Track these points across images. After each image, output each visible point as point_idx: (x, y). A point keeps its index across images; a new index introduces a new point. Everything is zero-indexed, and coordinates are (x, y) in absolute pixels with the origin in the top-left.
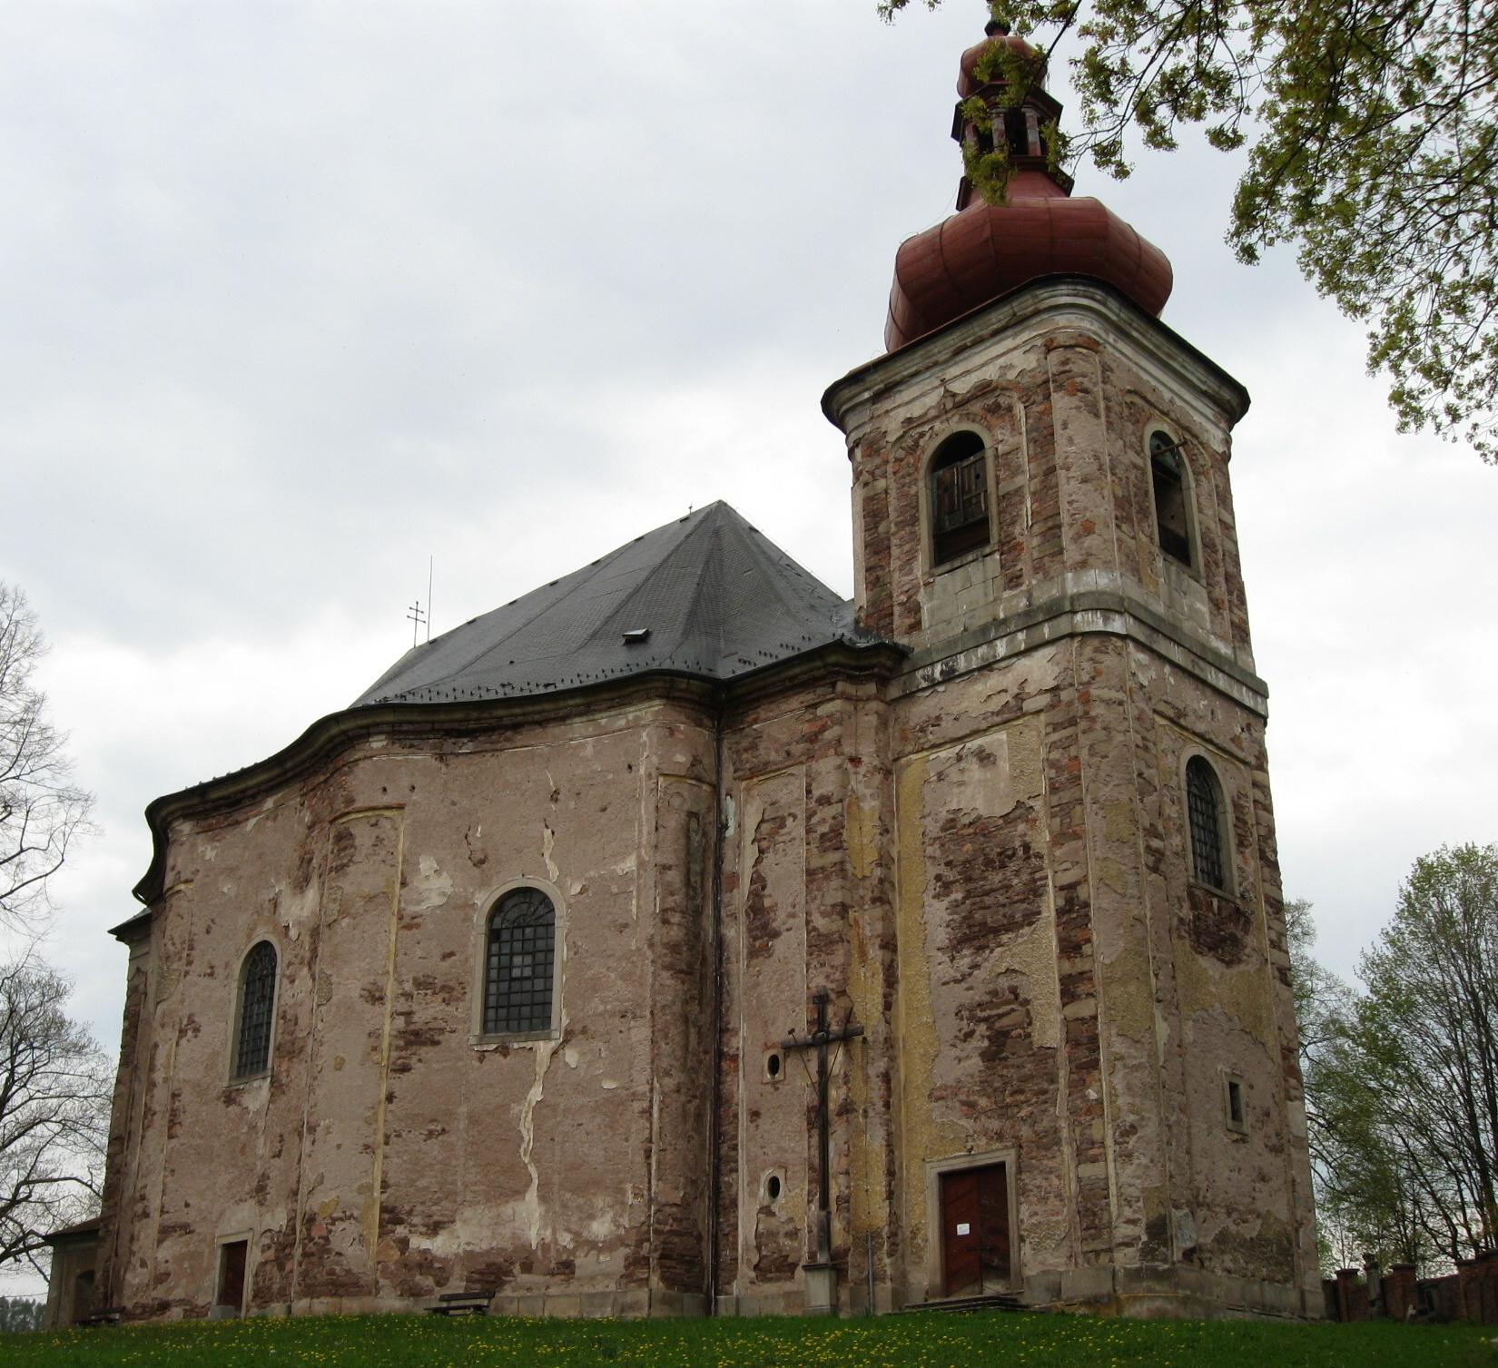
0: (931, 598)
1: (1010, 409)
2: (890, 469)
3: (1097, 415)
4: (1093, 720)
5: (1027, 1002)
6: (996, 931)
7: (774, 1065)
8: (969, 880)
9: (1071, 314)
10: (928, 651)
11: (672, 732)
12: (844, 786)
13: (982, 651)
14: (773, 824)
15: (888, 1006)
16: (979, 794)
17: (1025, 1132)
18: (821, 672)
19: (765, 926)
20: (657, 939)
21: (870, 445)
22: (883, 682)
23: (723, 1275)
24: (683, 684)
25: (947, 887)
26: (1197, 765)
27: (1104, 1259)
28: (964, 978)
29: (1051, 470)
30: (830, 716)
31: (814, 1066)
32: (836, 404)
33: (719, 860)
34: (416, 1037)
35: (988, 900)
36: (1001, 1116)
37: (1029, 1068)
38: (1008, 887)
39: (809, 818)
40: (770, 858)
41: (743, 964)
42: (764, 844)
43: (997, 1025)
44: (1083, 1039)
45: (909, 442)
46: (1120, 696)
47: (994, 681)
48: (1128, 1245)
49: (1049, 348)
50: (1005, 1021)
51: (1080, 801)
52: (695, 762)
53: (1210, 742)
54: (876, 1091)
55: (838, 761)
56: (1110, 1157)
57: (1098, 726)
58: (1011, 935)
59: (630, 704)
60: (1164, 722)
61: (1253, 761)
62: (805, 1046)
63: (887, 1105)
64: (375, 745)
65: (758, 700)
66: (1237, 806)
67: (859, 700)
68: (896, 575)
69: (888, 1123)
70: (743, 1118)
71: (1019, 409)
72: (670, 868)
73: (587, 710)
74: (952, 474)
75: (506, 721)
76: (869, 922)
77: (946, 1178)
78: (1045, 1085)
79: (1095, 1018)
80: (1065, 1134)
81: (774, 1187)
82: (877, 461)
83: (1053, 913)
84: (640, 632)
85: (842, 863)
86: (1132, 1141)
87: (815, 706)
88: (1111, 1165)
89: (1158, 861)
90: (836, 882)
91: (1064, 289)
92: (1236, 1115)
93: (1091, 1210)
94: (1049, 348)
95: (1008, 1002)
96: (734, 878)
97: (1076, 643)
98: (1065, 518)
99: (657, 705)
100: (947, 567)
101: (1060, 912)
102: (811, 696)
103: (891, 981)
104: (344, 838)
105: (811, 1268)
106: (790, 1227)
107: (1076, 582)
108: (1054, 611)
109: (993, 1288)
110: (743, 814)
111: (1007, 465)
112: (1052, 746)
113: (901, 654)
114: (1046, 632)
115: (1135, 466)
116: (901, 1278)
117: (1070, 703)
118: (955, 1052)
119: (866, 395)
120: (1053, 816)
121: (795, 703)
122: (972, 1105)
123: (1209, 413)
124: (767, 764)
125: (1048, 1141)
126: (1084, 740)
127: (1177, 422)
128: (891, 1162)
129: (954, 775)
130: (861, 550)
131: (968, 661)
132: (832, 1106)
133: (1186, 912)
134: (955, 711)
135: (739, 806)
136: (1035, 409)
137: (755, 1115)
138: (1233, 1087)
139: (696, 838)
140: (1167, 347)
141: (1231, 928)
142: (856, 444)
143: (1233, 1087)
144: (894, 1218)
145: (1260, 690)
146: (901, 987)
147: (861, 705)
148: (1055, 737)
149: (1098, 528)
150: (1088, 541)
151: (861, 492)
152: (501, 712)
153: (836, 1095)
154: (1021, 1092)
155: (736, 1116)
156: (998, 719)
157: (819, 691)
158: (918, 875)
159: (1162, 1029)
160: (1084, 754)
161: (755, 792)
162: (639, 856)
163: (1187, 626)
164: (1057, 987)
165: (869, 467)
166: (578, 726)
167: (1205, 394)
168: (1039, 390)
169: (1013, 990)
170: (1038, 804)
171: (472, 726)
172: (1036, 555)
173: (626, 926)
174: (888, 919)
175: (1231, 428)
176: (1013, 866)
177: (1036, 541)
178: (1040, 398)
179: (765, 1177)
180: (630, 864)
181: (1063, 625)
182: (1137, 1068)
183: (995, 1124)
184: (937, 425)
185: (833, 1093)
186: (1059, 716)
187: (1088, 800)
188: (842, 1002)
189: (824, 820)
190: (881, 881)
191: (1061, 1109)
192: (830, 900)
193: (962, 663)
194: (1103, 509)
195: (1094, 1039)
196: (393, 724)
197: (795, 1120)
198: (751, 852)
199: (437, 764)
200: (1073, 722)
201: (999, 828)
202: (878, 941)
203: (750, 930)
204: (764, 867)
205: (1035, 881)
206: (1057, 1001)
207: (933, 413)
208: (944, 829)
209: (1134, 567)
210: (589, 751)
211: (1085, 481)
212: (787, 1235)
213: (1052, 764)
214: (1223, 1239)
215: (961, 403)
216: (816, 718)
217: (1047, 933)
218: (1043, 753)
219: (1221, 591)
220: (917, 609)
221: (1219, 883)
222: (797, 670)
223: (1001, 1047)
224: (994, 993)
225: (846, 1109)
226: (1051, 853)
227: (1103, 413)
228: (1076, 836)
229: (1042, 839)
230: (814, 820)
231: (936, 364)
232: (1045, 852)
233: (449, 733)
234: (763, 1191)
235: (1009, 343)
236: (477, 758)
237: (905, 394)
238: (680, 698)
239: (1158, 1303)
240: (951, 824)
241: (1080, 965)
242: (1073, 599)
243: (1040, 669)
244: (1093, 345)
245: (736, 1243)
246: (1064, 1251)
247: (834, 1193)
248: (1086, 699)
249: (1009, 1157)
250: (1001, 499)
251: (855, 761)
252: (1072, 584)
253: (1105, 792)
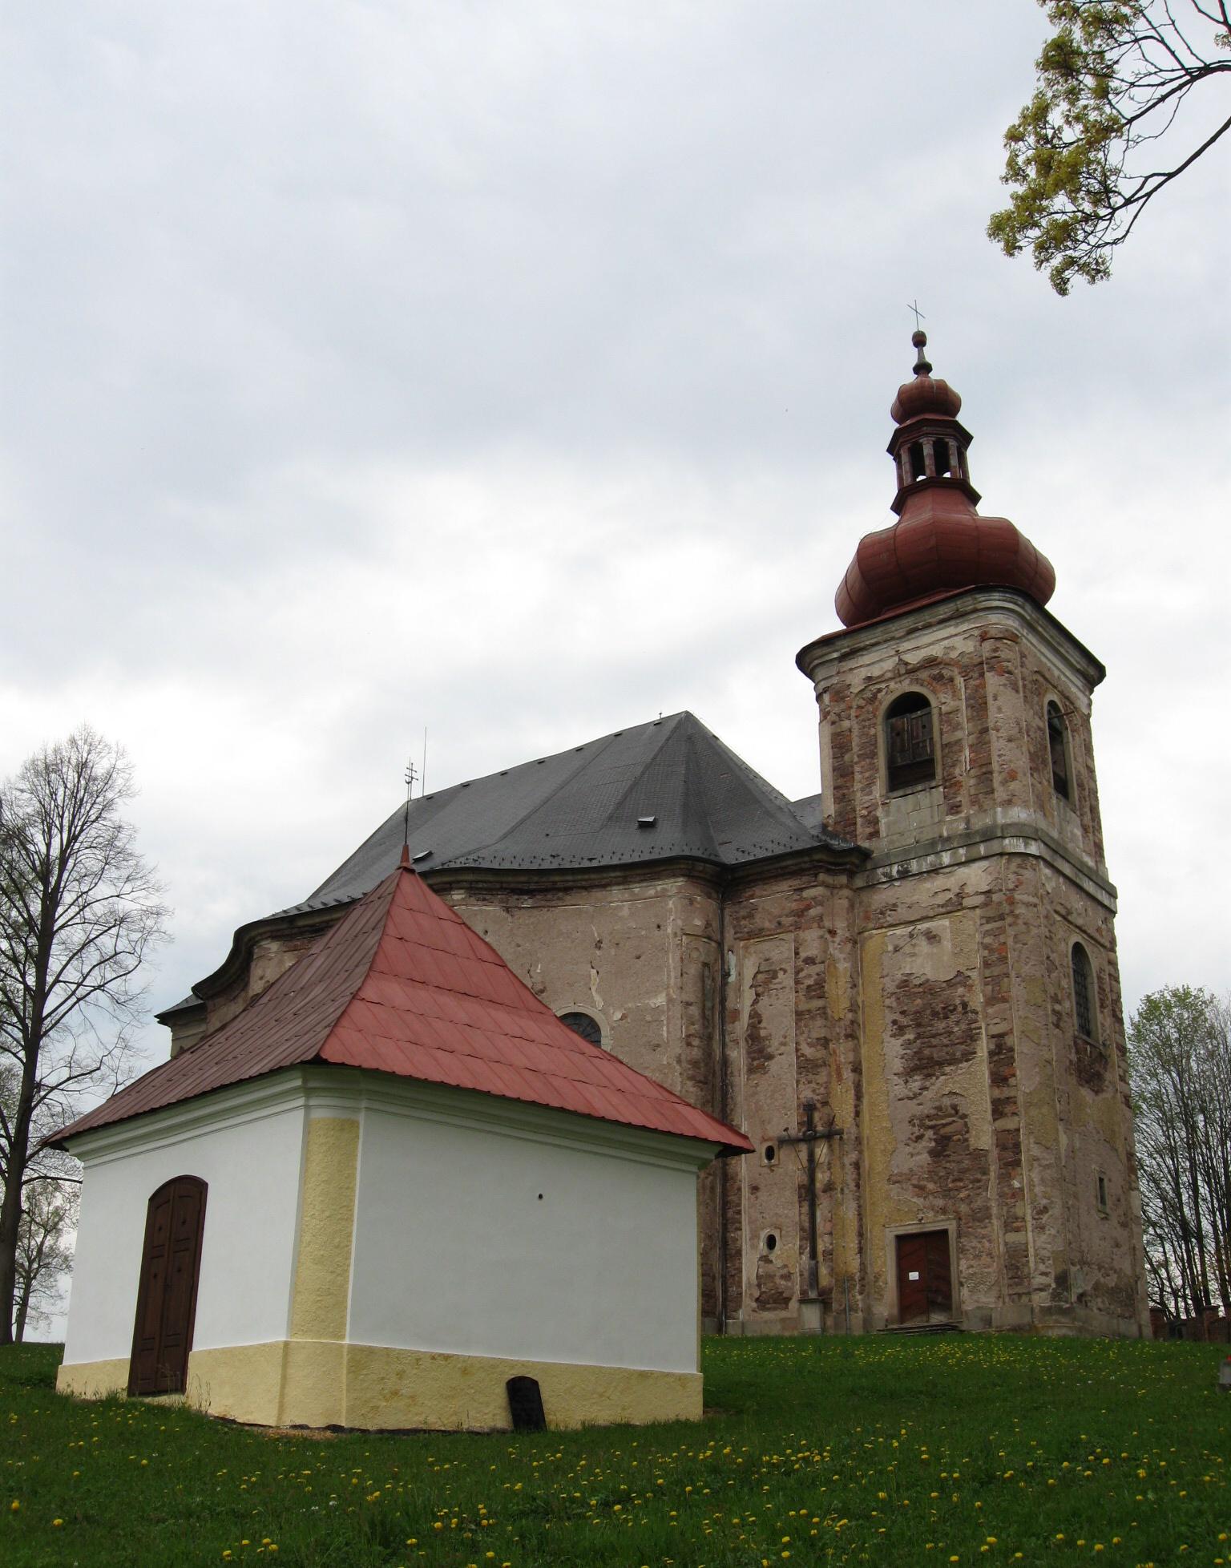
0: (888, 814)
1: (951, 680)
2: (853, 713)
3: (1017, 691)
4: (1017, 917)
5: (964, 1116)
6: (940, 1064)
7: (770, 1154)
8: (919, 1025)
9: (999, 613)
10: (888, 855)
11: (691, 902)
12: (825, 952)
13: (930, 859)
14: (766, 977)
15: (857, 1114)
16: (927, 964)
17: (963, 1208)
18: (807, 866)
19: (761, 1051)
20: (683, 1057)
21: (838, 692)
22: (851, 874)
23: (731, 1305)
24: (700, 866)
25: (901, 1030)
26: (1078, 947)
27: (1024, 1299)
28: (915, 1096)
29: (985, 730)
30: (814, 898)
31: (804, 1156)
32: (807, 660)
33: (723, 1000)
35: (934, 1041)
36: (944, 1197)
37: (967, 1163)
38: (951, 1033)
39: (797, 973)
40: (764, 1001)
41: (743, 1078)
42: (760, 990)
43: (942, 1131)
44: (1009, 1145)
45: (869, 695)
47: (939, 882)
48: (1041, 1290)
49: (984, 638)
50: (948, 1129)
51: (1007, 975)
52: (708, 925)
53: (1085, 932)
54: (850, 1176)
55: (821, 932)
56: (1030, 1228)
57: (1020, 921)
59: (659, 879)
60: (1059, 918)
61: (1107, 944)
62: (799, 1140)
63: (858, 1186)
64: (456, 897)
65: (755, 881)
66: (1099, 978)
67: (834, 887)
68: (859, 794)
69: (858, 1198)
70: (745, 1192)
71: (960, 681)
73: (624, 882)
74: (904, 722)
75: (559, 885)
76: (843, 1051)
77: (900, 1239)
78: (979, 1176)
79: (1018, 1130)
80: (994, 1211)
81: (771, 1242)
82: (843, 706)
83: (986, 1054)
84: (651, 819)
85: (824, 1008)
86: (1045, 1217)
87: (802, 890)
88: (1030, 1234)
89: (1059, 1019)
90: (819, 1022)
91: (996, 595)
92: (1103, 1201)
93: (1015, 1265)
94: (984, 638)
95: (951, 1116)
96: (736, 1014)
97: (1004, 860)
98: (995, 766)
99: (680, 882)
100: (901, 793)
101: (991, 1054)
102: (798, 882)
103: (859, 1096)
105: (804, 1301)
106: (785, 1271)
107: (1005, 814)
108: (988, 835)
109: (937, 1318)
110: (743, 966)
111: (949, 722)
112: (987, 933)
113: (865, 855)
114: (982, 849)
115: (1039, 728)
116: (868, 1310)
117: (999, 904)
118: (908, 1149)
119: (835, 655)
120: (987, 984)
121: (785, 886)
122: (922, 1188)
123: (1080, 684)
124: (761, 930)
125: (982, 1216)
126: (1011, 931)
128: (861, 1226)
129: (907, 949)
130: (830, 775)
131: (920, 865)
132: (818, 1185)
133: (1074, 1057)
134: (909, 901)
135: (738, 959)
136: (972, 682)
137: (755, 1189)
138: (1101, 1180)
139: (708, 982)
140: (1054, 632)
141: (1097, 1067)
142: (825, 691)
143: (1101, 1180)
144: (863, 1267)
145: (1112, 893)
146: (865, 1100)
148: (988, 927)
149: (1020, 776)
150: (1013, 785)
151: (829, 729)
152: (557, 878)
153: (821, 1177)
154: (960, 1180)
155: (739, 1189)
157: (805, 879)
158: (879, 1020)
159: (1064, 1139)
160: (1010, 942)
161: (752, 950)
162: (668, 995)
163: (1070, 846)
164: (989, 1107)
165: (836, 710)
166: (616, 892)
167: (1078, 671)
168: (976, 669)
169: (954, 1107)
170: (974, 974)
171: (532, 887)
172: (973, 792)
173: (658, 1046)
174: (856, 1050)
175: (1091, 692)
176: (953, 1018)
177: (972, 782)
178: (976, 675)
179: (764, 1234)
180: (660, 1000)
181: (995, 846)
182: (1048, 1166)
183: (940, 1202)
184: (892, 685)
185: (819, 1176)
186: (991, 913)
187: (1013, 974)
188: (826, 1110)
189: (810, 976)
190: (852, 1022)
191: (992, 1192)
192: (815, 1035)
193: (914, 866)
194: (1022, 762)
195: (1017, 1145)
196: (471, 882)
197: (787, 1193)
198: (749, 996)
199: (505, 914)
200: (1002, 917)
201: (943, 989)
202: (850, 1067)
203: (749, 1053)
204: (760, 1007)
205: (971, 1030)
206: (989, 1117)
207: (889, 675)
208: (898, 987)
209: (1041, 807)
210: (625, 912)
211: (1010, 740)
212: (782, 1277)
213: (986, 947)
214: (1097, 1287)
215: (912, 671)
216: (802, 899)
217: (981, 1067)
218: (978, 937)
219: (1088, 818)
220: (875, 821)
221: (1088, 1034)
222: (789, 862)
223: (944, 1147)
224: (939, 1108)
225: (829, 1188)
226: (984, 1010)
228: (1004, 1000)
229: (977, 1000)
230: (802, 975)
231: (893, 638)
232: (979, 1009)
233: (514, 891)
234: (762, 1245)
235: (951, 630)
236: (535, 912)
237: (866, 659)
239: (1064, 1331)
240: (904, 984)
241: (1007, 1092)
242: (1004, 827)
243: (977, 877)
244: (1014, 638)
245: (740, 1282)
246: (994, 1293)
247: (820, 1247)
248: (1011, 902)
249: (951, 1227)
250: (944, 746)
251: (832, 933)
252: (1001, 817)
253: (1026, 970)
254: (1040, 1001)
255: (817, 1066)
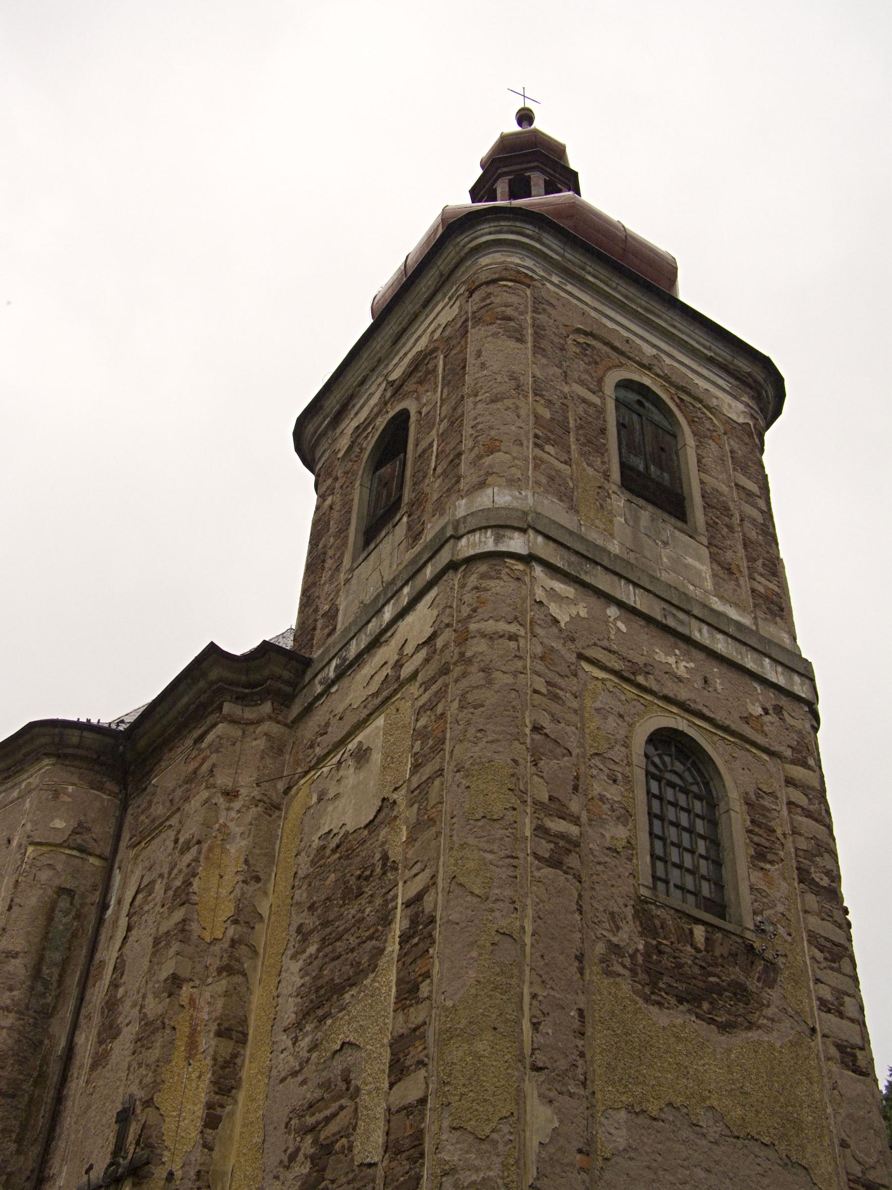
4: (470, 661)
11: (56, 794)
15: (212, 1121)
22: (284, 700)
46: (513, 628)
52: (80, 829)
58: (354, 991)
72: (16, 955)
127: (666, 378)
139: (62, 921)
141: (735, 973)
145: (806, 673)
147: (251, 728)
156: (377, 701)
159: (540, 1119)
167: (710, 360)
174: (238, 996)
181: (444, 557)
188: (150, 1116)
190: (233, 943)
202: (214, 1027)
227: (529, 339)
238: (74, 757)
244: (521, 279)
254: (497, 809)
255: (111, 1027)
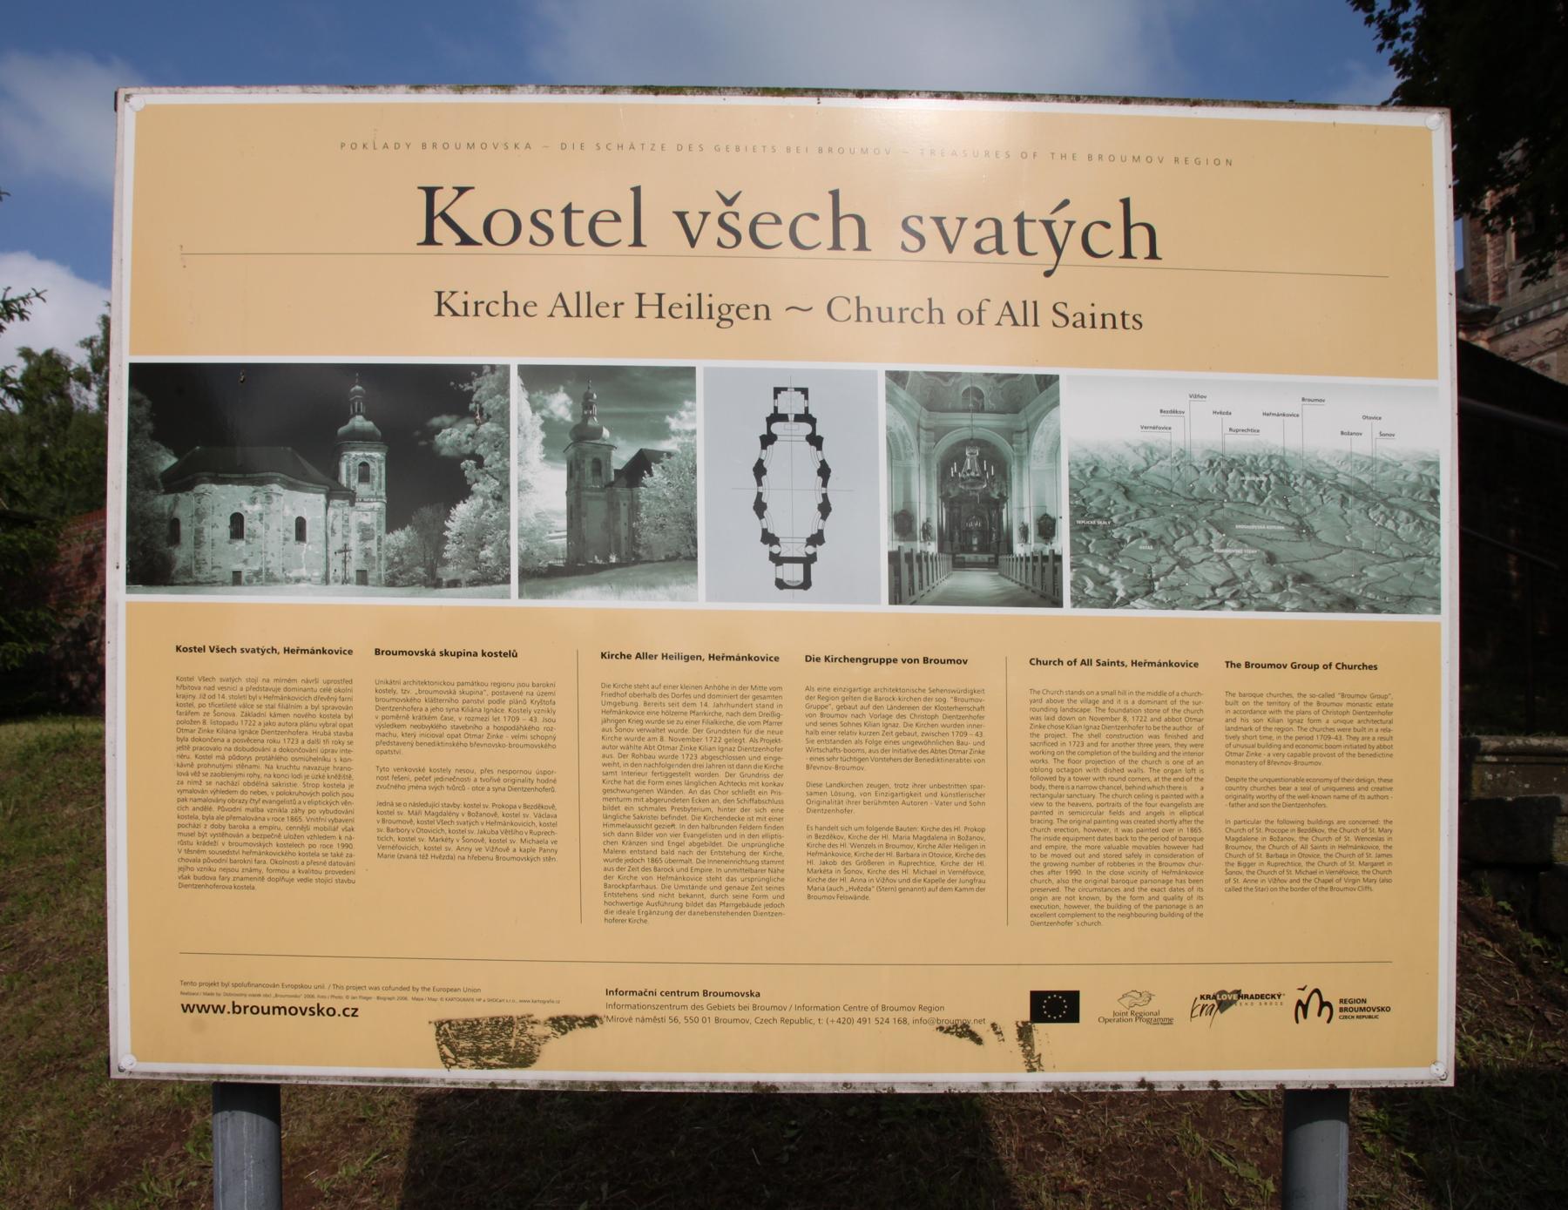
14: (336, 516)
16: (367, 520)
34: (286, 539)
104: (268, 497)
217: (375, 541)
